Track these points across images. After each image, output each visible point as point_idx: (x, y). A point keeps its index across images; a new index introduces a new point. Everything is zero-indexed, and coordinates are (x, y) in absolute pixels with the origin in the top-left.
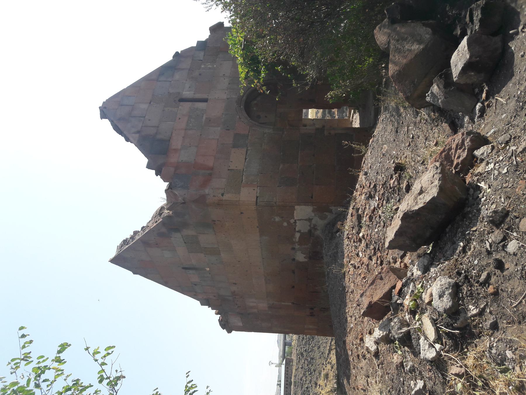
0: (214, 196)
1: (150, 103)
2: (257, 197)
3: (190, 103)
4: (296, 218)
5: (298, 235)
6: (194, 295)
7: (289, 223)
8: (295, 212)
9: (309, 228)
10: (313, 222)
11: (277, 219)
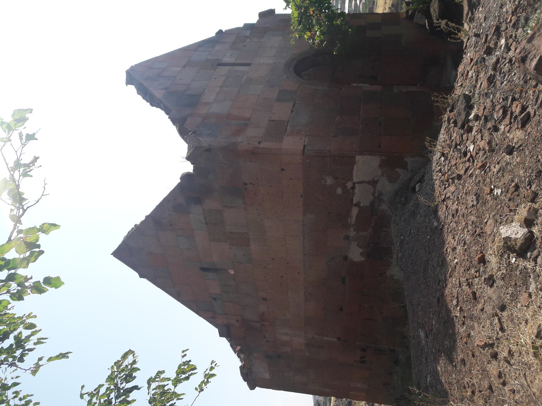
0: (248, 144)
1: (184, 67)
2: (305, 146)
3: (230, 67)
4: (355, 180)
5: (355, 211)
6: (212, 320)
7: (344, 187)
8: (355, 167)
9: (371, 198)
10: (379, 187)
11: (329, 181)
